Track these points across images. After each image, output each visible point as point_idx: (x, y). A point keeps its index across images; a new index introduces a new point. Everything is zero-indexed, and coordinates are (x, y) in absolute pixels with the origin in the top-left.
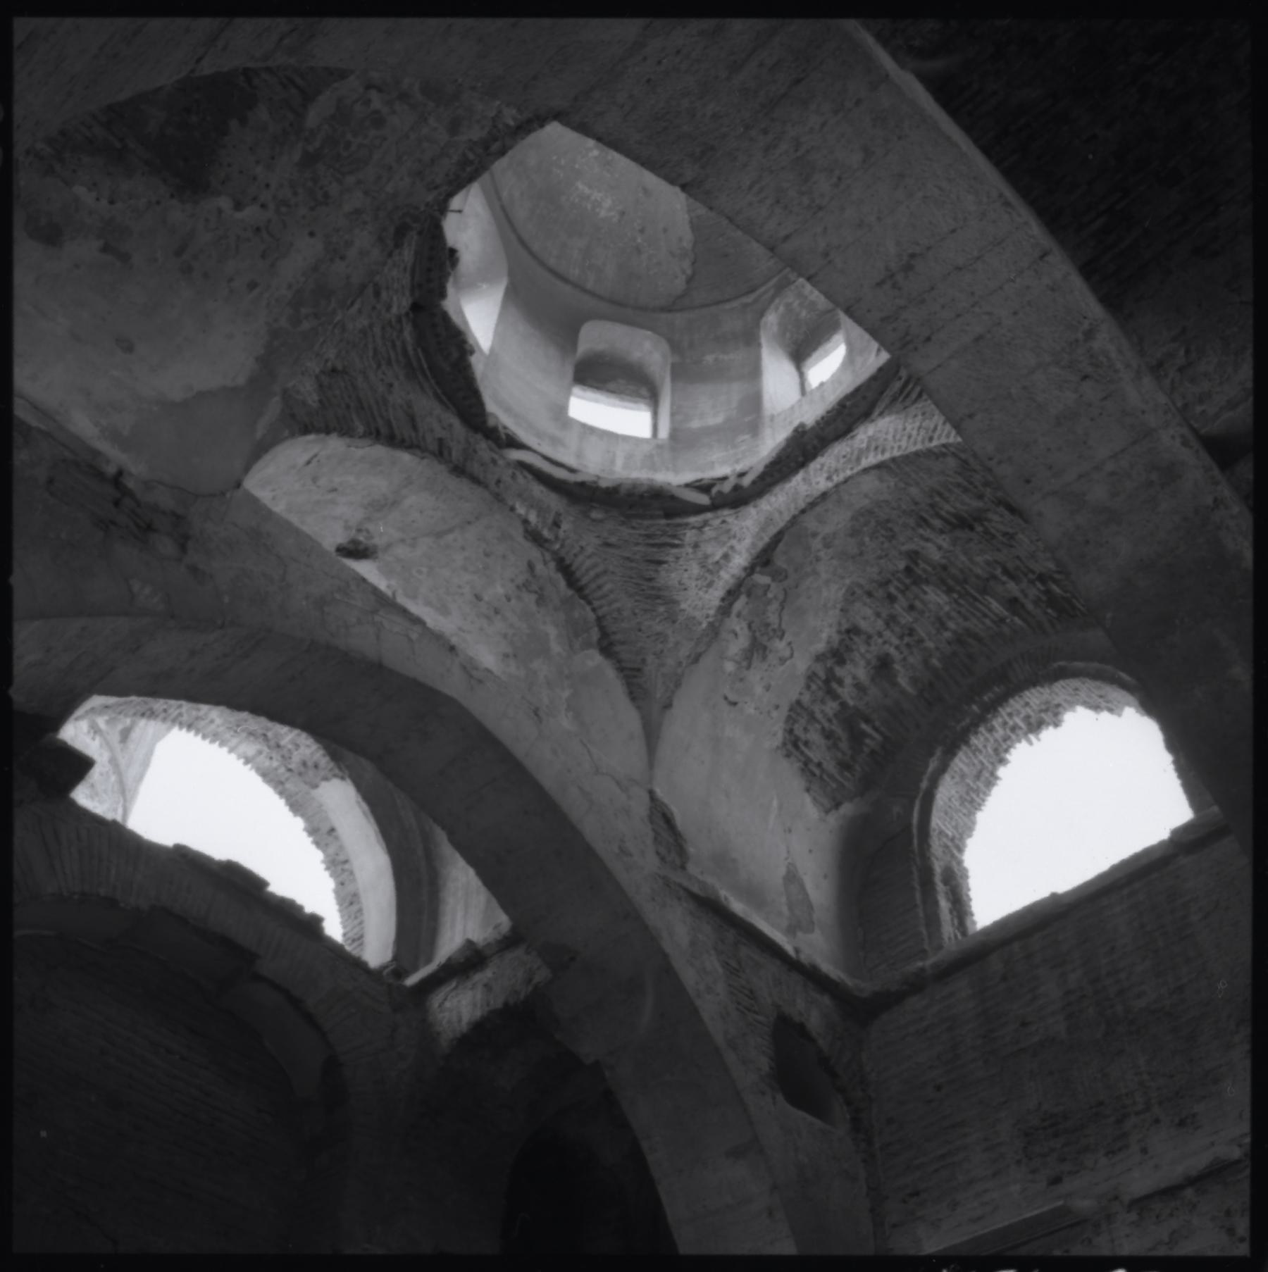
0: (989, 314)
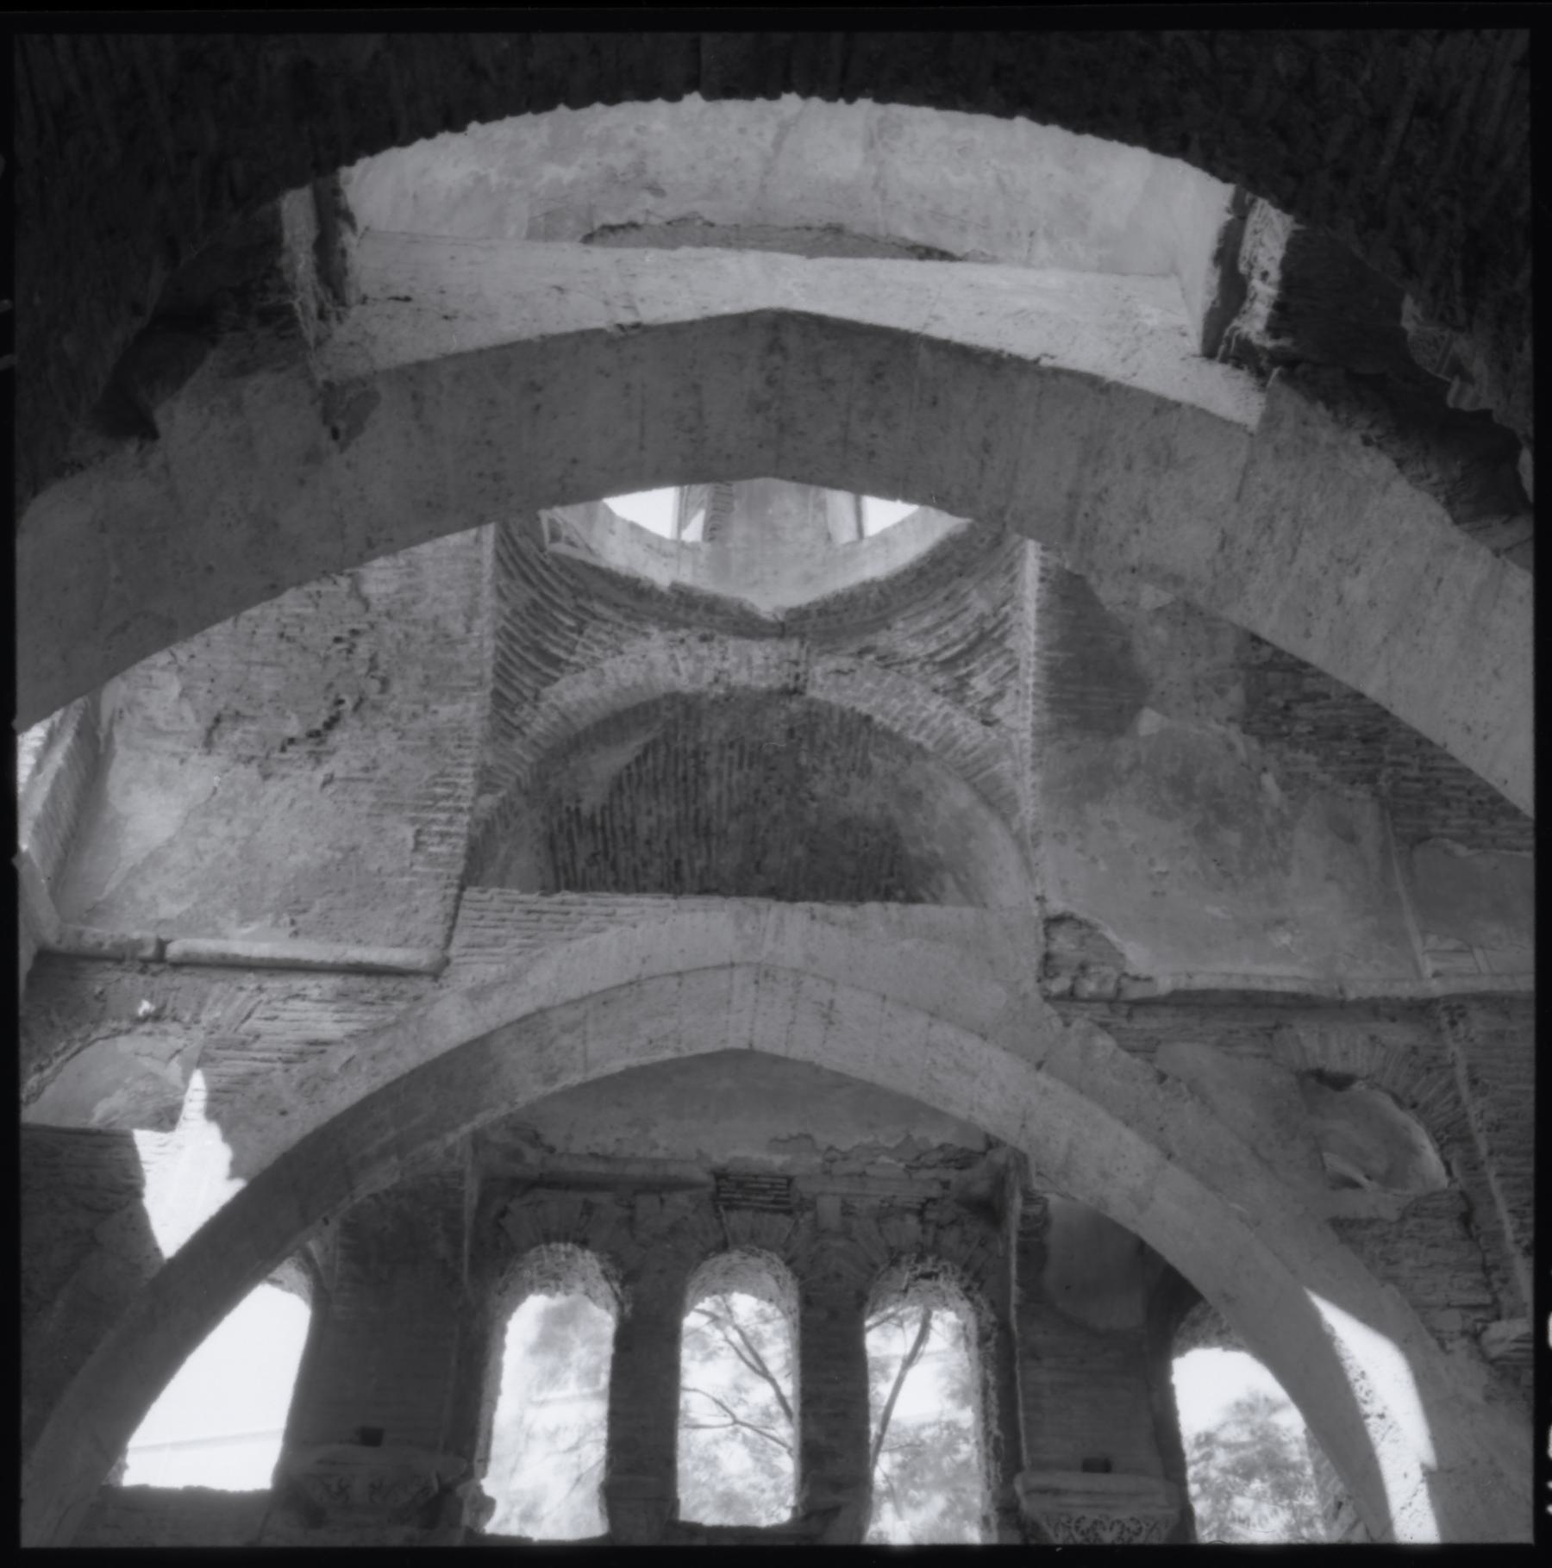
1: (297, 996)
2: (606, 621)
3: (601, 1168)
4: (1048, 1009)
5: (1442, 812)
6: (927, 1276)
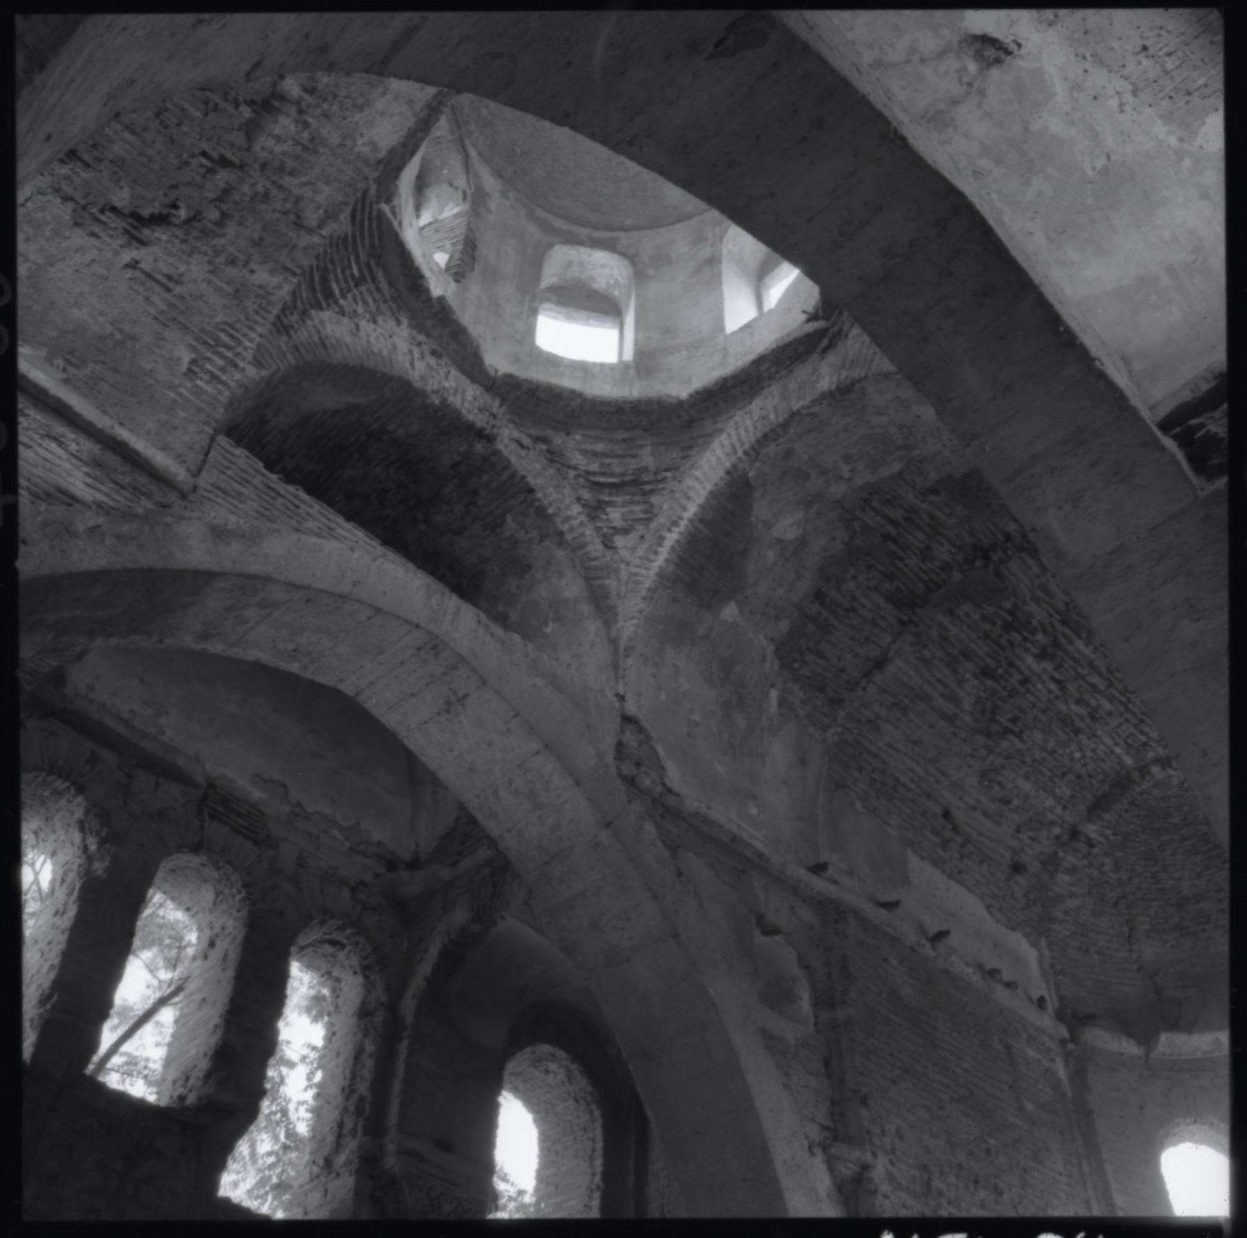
0: (380, 664)
1: (55, 439)
2: (378, 289)
3: (121, 729)
4: (619, 782)
5: (857, 774)
6: (333, 943)
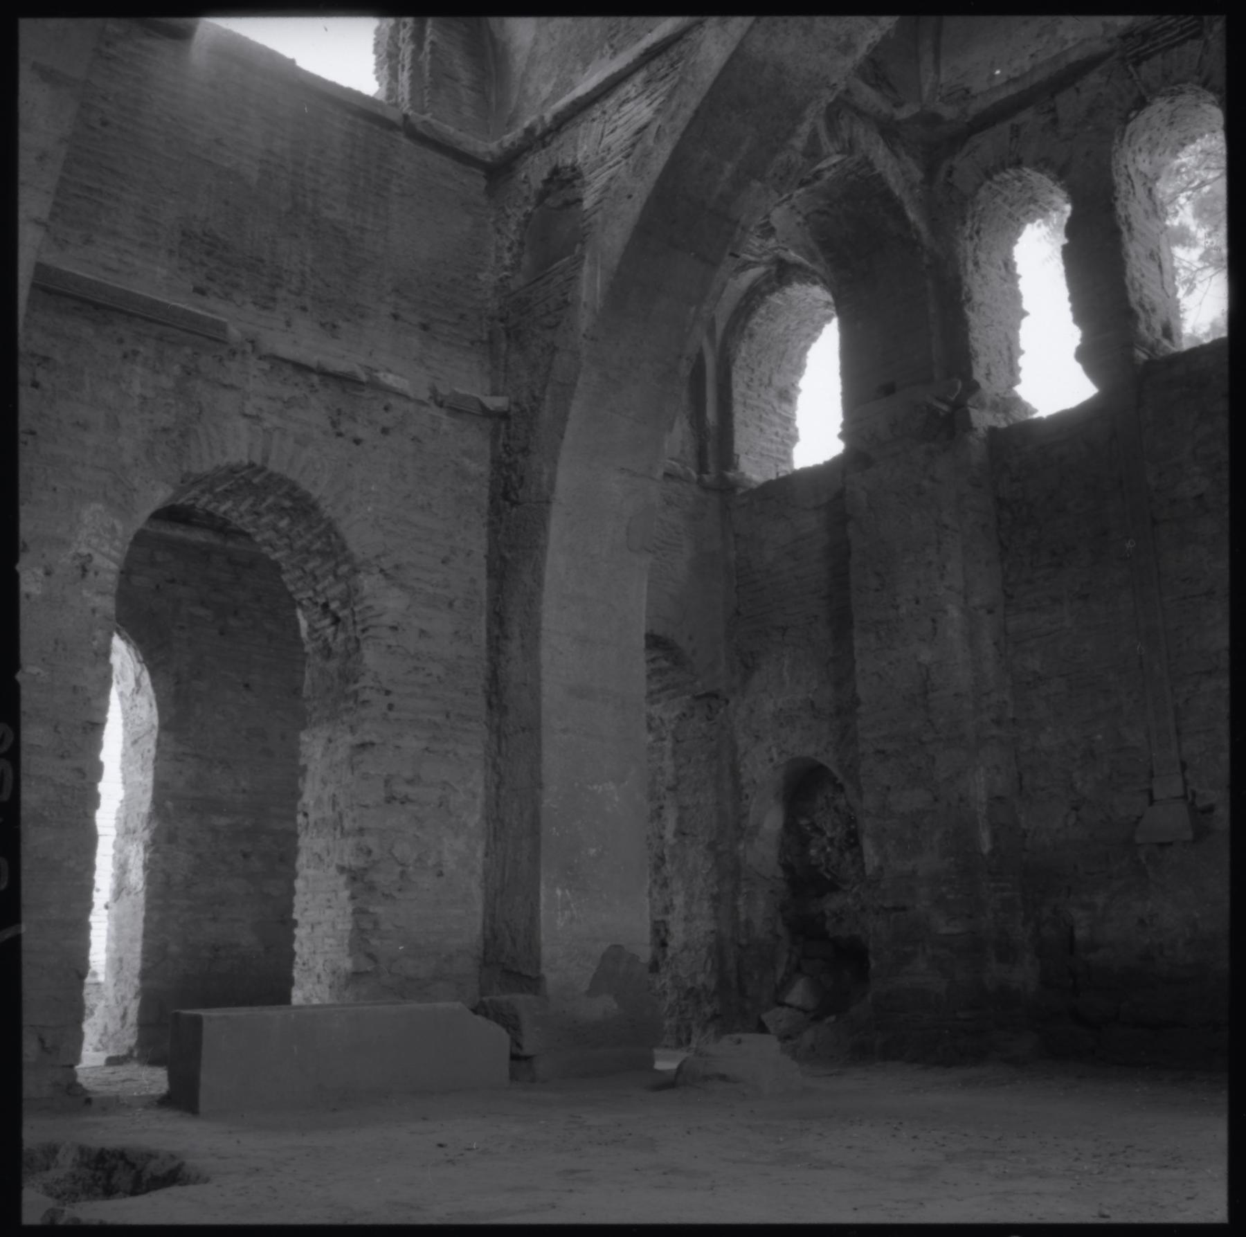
3: (1012, 90)
